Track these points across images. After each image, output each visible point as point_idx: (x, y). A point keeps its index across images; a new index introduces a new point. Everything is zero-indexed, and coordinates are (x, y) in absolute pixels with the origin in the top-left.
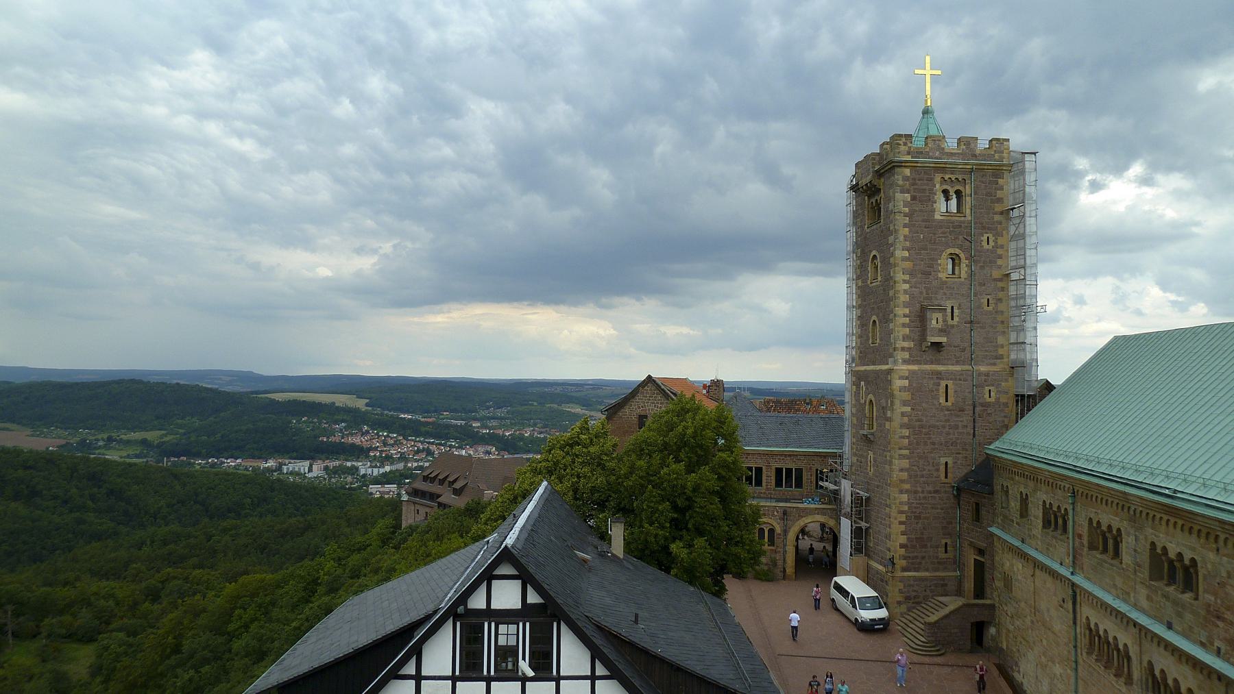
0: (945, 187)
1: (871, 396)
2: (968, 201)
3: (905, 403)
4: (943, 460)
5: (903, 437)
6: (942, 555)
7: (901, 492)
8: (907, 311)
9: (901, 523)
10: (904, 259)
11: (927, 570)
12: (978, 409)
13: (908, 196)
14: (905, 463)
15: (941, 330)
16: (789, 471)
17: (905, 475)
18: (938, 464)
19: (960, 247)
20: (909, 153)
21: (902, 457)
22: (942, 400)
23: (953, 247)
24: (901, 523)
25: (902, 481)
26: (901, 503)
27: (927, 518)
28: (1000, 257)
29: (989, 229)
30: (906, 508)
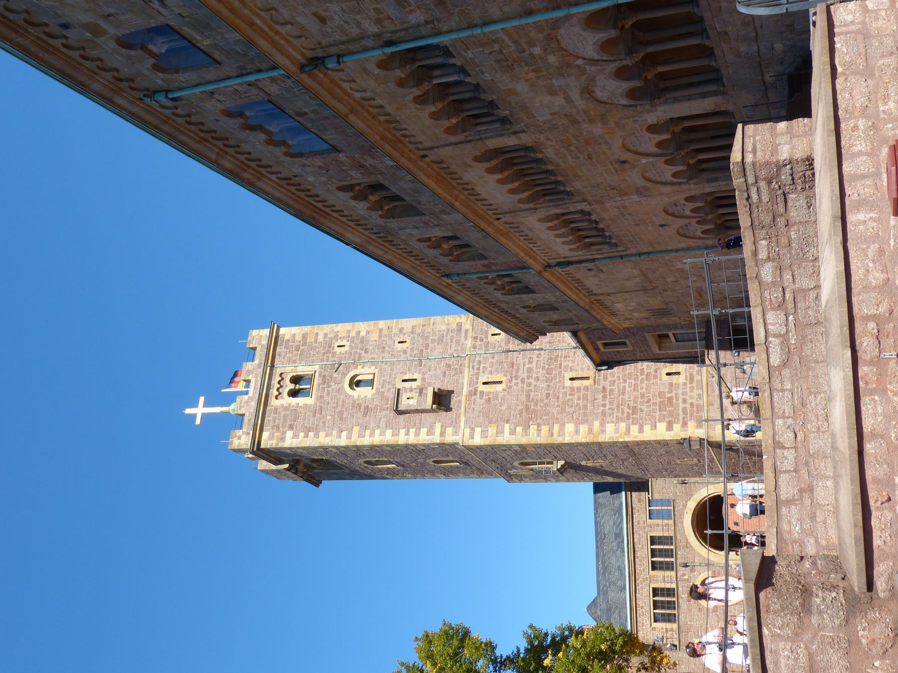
0: (285, 394)
1: (516, 464)
2: (302, 369)
3: (500, 432)
4: (568, 383)
5: (539, 431)
6: (681, 379)
7: (603, 431)
8: (403, 432)
9: (641, 431)
10: (349, 437)
11: (700, 396)
12: (511, 346)
13: (289, 434)
14: (570, 427)
15: (421, 394)
16: (654, 553)
17: (583, 428)
18: (572, 389)
19: (344, 375)
20: (249, 433)
21: (561, 432)
22: (499, 388)
23: (341, 382)
24: (641, 431)
25: (590, 431)
26: (617, 431)
27: (635, 401)
28: (358, 333)
29: (330, 346)
30: (623, 425)
